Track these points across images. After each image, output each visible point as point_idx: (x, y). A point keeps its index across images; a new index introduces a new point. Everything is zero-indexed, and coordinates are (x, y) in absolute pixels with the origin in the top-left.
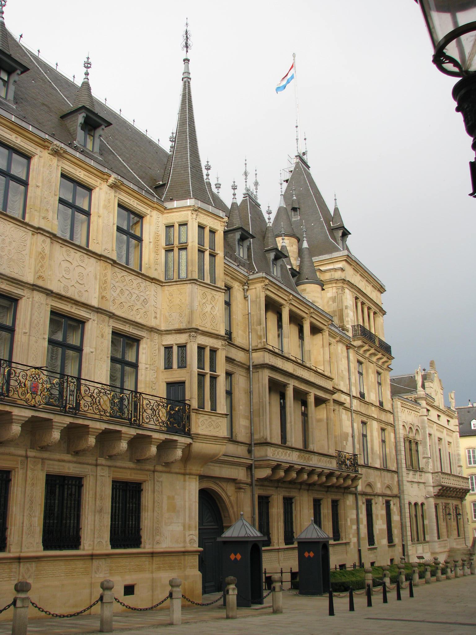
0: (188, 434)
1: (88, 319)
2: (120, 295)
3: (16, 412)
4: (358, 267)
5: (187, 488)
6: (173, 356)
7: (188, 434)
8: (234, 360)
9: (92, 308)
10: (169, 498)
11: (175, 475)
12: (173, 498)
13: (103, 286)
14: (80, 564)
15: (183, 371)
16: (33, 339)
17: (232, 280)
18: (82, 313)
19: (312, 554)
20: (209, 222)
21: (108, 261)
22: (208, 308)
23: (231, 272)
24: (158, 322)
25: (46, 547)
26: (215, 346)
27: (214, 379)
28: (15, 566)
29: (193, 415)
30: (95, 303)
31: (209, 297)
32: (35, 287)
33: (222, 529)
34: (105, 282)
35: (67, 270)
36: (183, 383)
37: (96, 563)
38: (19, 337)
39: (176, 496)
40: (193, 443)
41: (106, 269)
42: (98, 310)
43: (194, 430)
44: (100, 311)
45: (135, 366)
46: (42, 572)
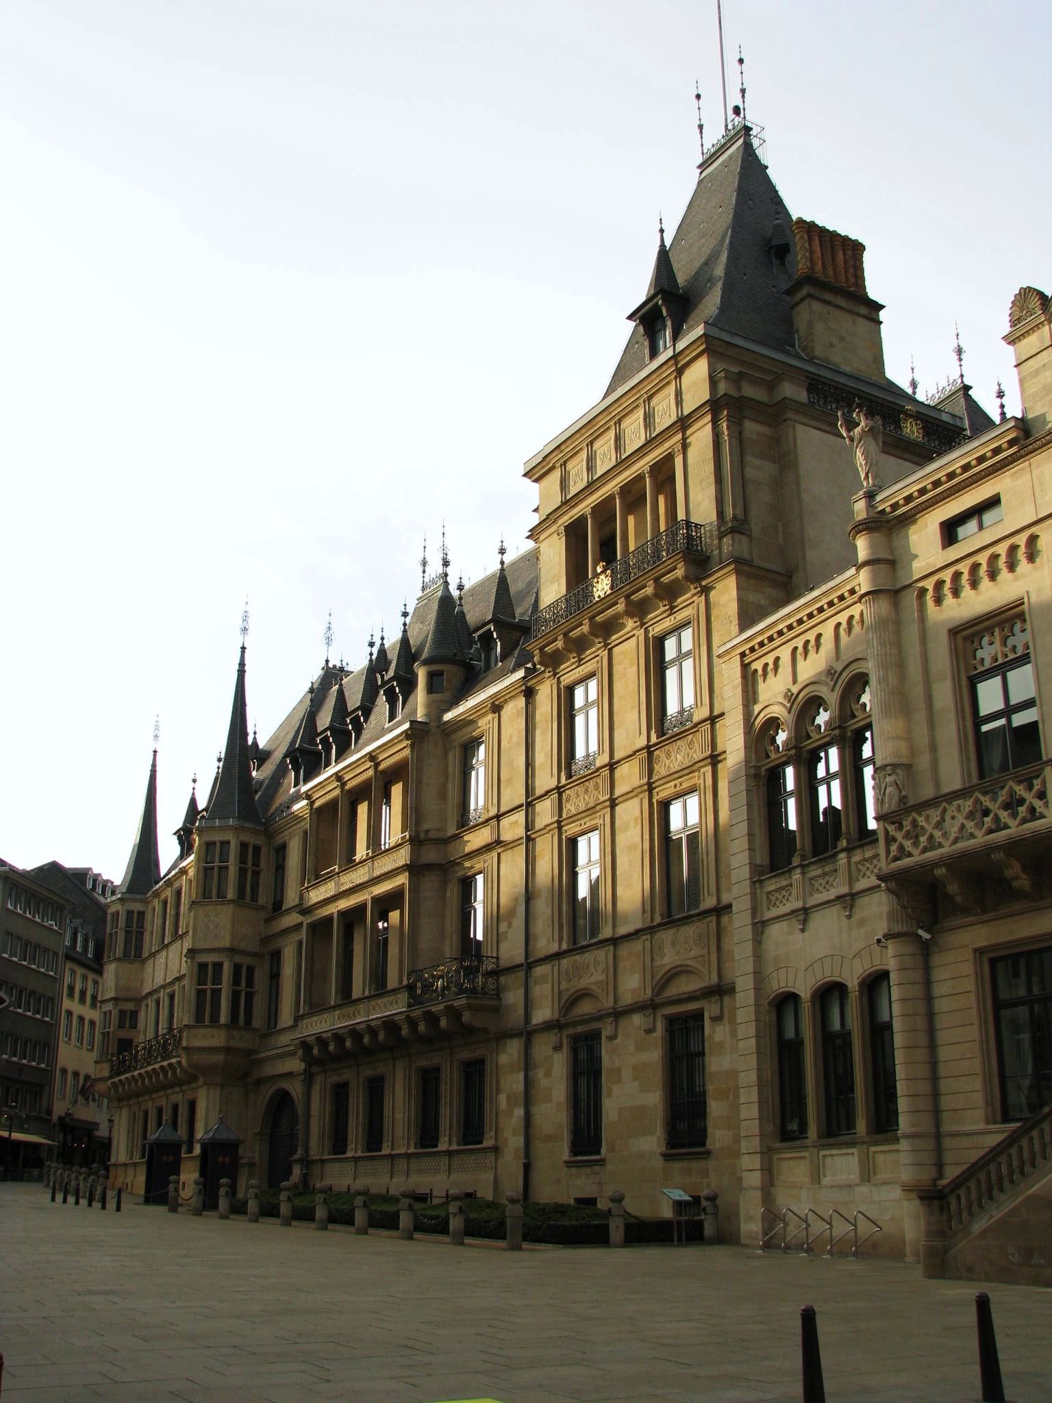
4: (567, 449)
19: (227, 1160)
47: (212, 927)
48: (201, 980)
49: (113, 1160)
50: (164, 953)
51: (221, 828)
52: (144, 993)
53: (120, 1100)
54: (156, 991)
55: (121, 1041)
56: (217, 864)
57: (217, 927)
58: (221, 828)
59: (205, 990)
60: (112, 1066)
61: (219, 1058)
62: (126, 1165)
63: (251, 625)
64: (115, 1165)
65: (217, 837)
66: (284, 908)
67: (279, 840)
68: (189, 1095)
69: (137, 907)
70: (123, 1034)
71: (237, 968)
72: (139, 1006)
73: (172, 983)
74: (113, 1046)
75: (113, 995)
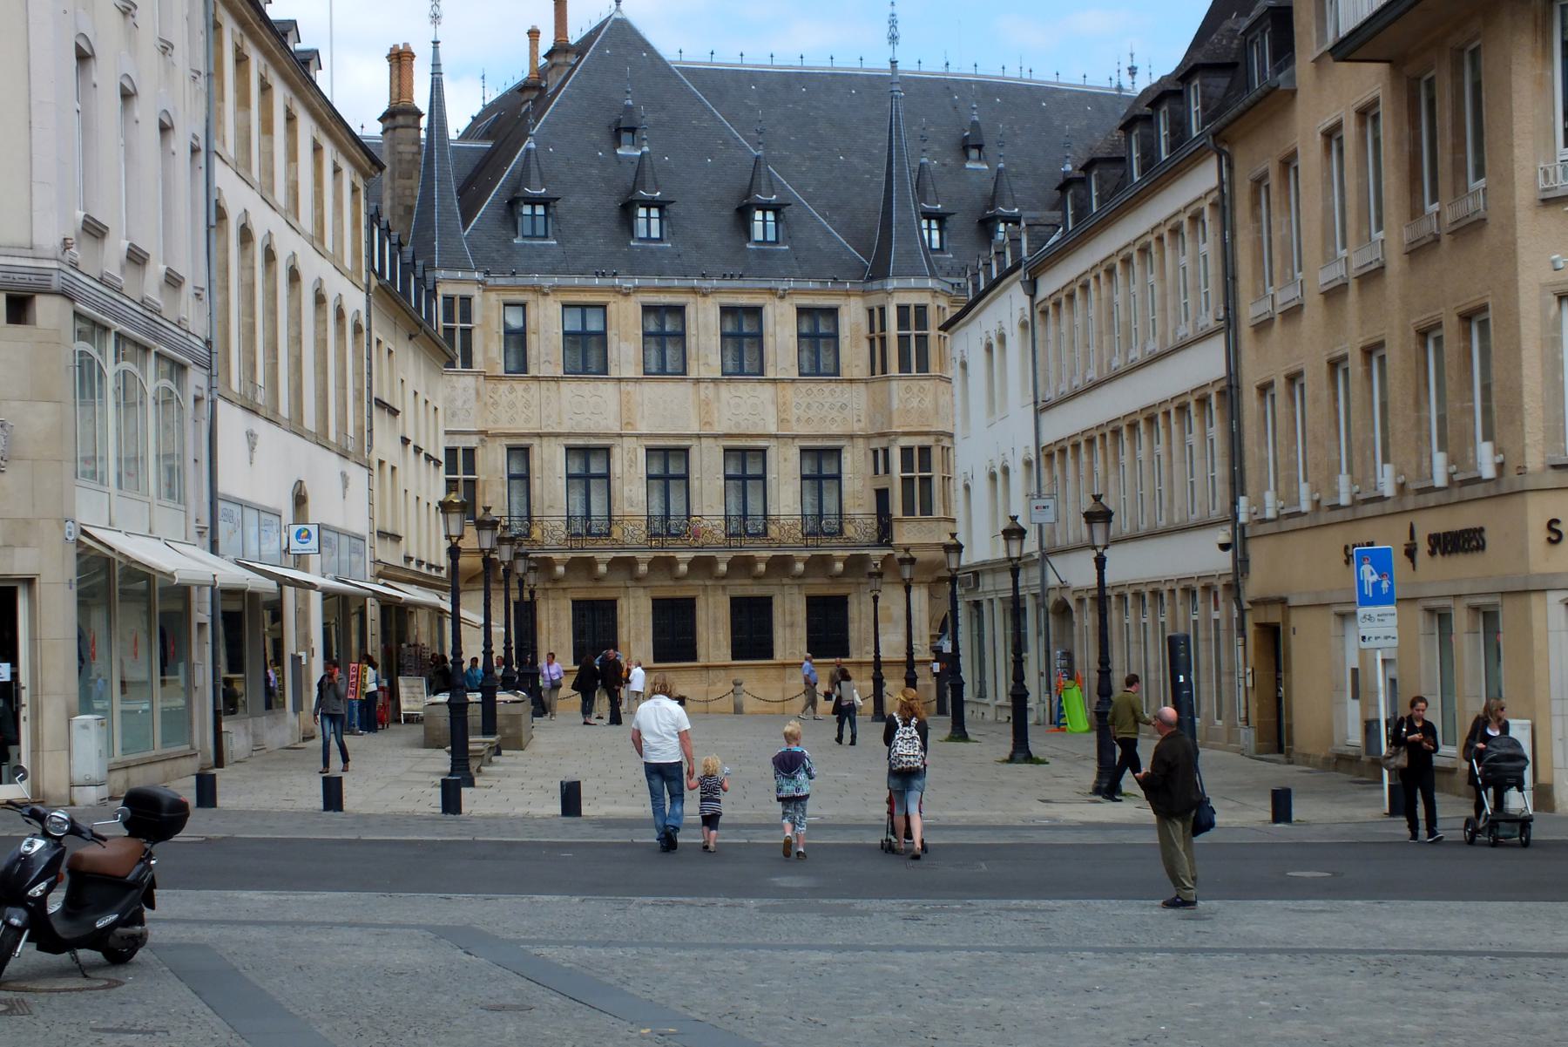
0: (889, 545)
3: (679, 555)
6: (880, 459)
7: (889, 545)
13: (781, 407)
14: (773, 673)
15: (886, 478)
16: (705, 482)
18: (761, 443)
20: (912, 299)
22: (915, 403)
24: (862, 425)
25: (734, 658)
27: (926, 481)
28: (704, 673)
29: (895, 526)
30: (773, 430)
31: (915, 390)
32: (699, 436)
35: (738, 405)
36: (886, 491)
37: (788, 671)
38: (694, 483)
42: (776, 436)
43: (896, 542)
45: (838, 477)
48: (907, 464)
59: (912, 479)
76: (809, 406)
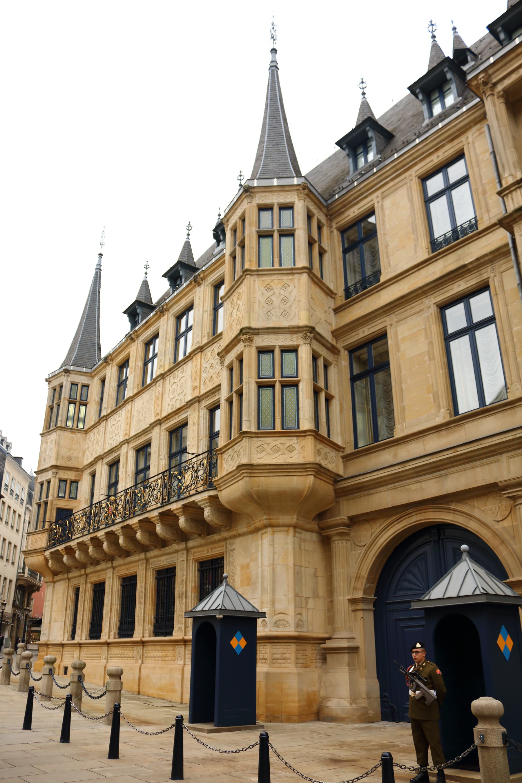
1: (186, 418)
2: (211, 371)
5: (260, 549)
8: (464, 266)
9: (183, 408)
10: (242, 567)
11: (250, 536)
12: (248, 566)
14: (169, 650)
17: (456, 142)
21: (196, 352)
23: (438, 140)
26: (239, 352)
33: (376, 599)
34: (196, 372)
39: (251, 564)
40: (219, 493)
41: (197, 360)
44: (189, 404)
46: (149, 655)
47: (276, 301)
49: (43, 639)
50: (123, 413)
51: (282, 188)
52: (86, 462)
53: (55, 574)
54: (111, 451)
55: (60, 511)
56: (276, 227)
57: (284, 301)
58: (282, 188)
60: (50, 536)
61: (304, 482)
62: (63, 645)
63: (278, 35)
64: (47, 645)
65: (275, 199)
66: (383, 279)
67: (353, 212)
68: (207, 553)
69: (82, 380)
70: (63, 504)
71: (315, 358)
72: (81, 476)
73: (146, 431)
74: (51, 515)
75: (54, 463)
76: (212, 366)
